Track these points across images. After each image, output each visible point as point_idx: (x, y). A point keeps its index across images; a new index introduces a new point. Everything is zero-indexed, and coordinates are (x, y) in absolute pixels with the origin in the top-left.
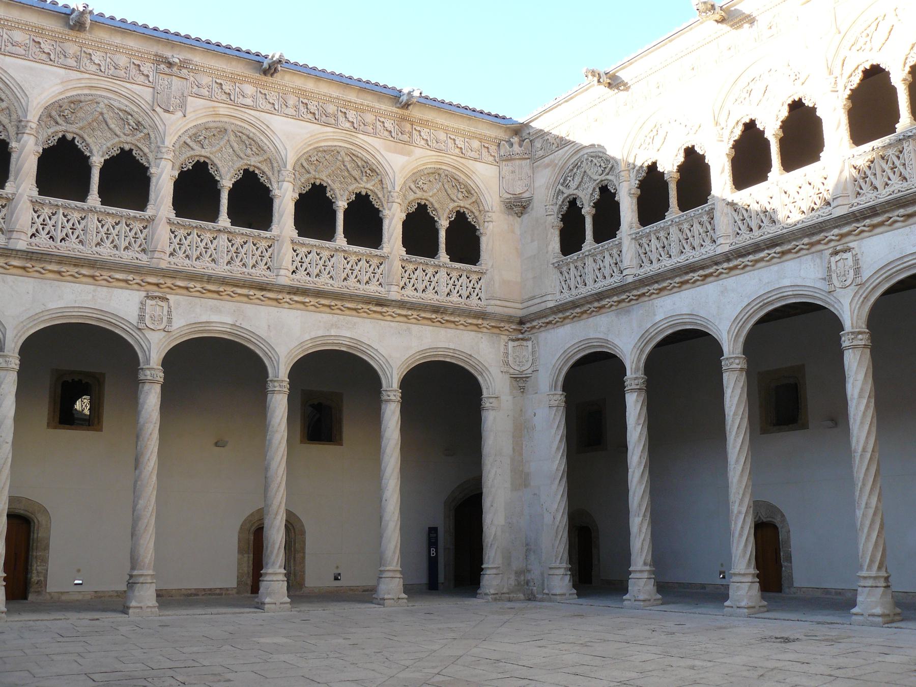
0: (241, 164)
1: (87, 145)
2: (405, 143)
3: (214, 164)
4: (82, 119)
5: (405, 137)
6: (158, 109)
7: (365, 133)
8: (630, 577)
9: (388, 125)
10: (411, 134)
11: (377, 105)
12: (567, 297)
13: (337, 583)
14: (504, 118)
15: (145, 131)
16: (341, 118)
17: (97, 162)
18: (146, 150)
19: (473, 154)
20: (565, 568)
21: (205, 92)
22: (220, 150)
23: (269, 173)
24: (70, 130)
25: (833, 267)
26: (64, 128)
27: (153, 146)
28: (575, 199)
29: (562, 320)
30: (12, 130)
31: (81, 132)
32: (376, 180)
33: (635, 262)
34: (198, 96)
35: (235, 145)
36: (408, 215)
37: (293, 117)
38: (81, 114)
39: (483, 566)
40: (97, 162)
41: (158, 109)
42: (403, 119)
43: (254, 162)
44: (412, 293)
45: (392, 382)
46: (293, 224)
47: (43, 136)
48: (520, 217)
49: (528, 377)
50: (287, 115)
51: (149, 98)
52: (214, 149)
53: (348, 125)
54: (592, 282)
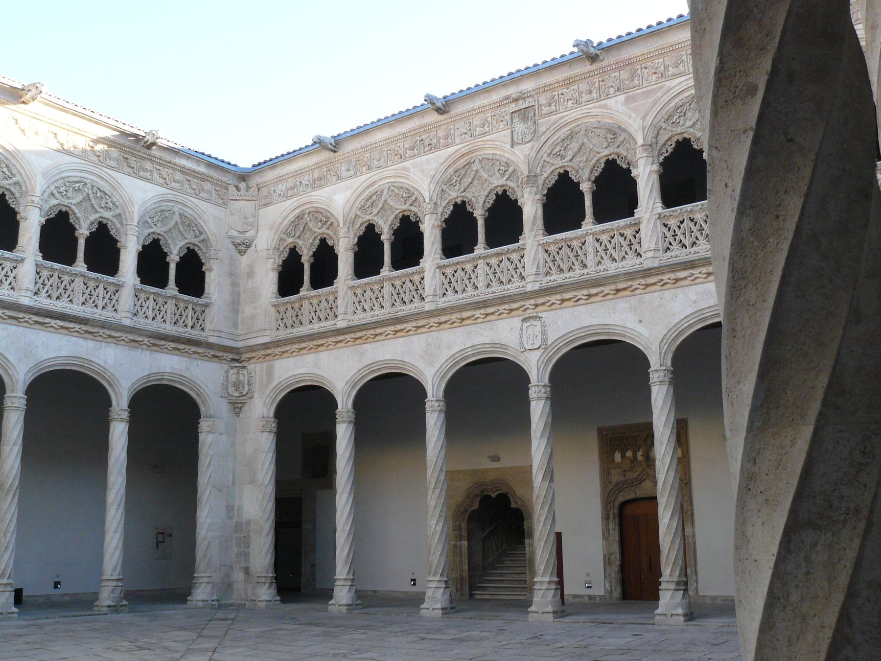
8: (336, 584)
10: (151, 172)
12: (283, 334)
13: (57, 591)
14: (236, 166)
20: (271, 577)
25: (524, 331)
28: (295, 247)
29: (281, 353)
33: (351, 309)
36: (144, 247)
39: (195, 575)
44: (143, 320)
45: (120, 403)
46: (38, 247)
48: (242, 255)
49: (244, 403)
54: (308, 322)
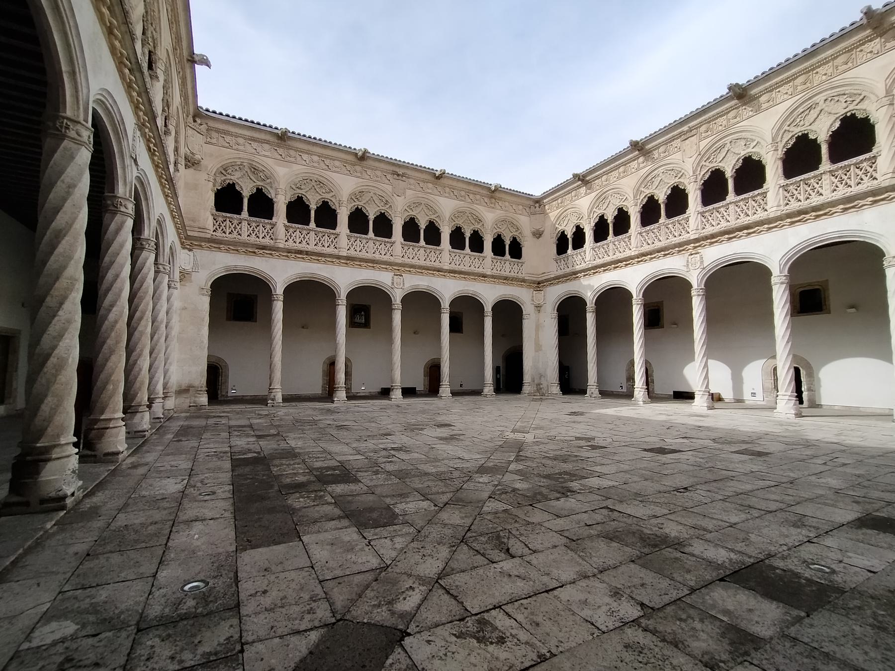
0: (427, 218)
1: (367, 211)
2: (493, 208)
3: (417, 219)
4: (364, 199)
5: (493, 205)
6: (394, 195)
7: (476, 204)
9: (486, 200)
11: (481, 191)
15: (390, 204)
16: (467, 197)
17: (372, 217)
18: (390, 213)
19: (520, 212)
21: (412, 187)
22: (419, 213)
23: (439, 222)
24: (360, 204)
26: (356, 204)
27: (393, 211)
30: (337, 205)
31: (364, 205)
32: (481, 224)
34: (410, 189)
35: (426, 211)
37: (447, 197)
38: (363, 197)
40: (372, 217)
41: (394, 195)
42: (492, 197)
43: (433, 217)
47: (349, 208)
50: (446, 197)
51: (391, 190)
52: (417, 212)
53: (470, 200)
